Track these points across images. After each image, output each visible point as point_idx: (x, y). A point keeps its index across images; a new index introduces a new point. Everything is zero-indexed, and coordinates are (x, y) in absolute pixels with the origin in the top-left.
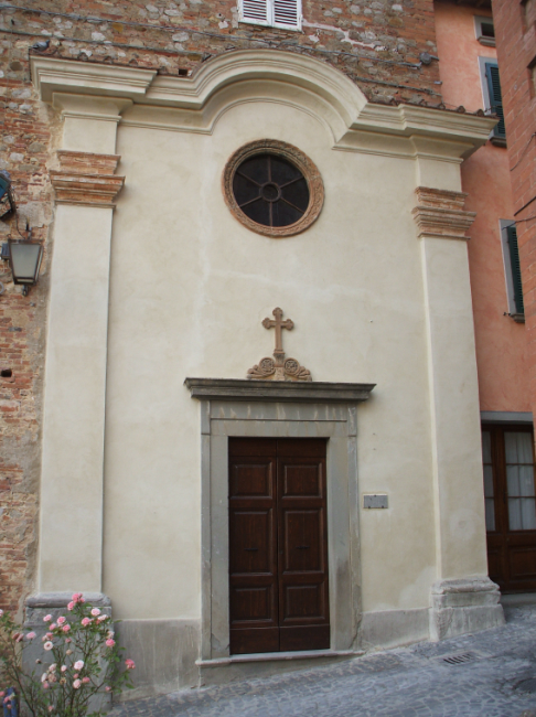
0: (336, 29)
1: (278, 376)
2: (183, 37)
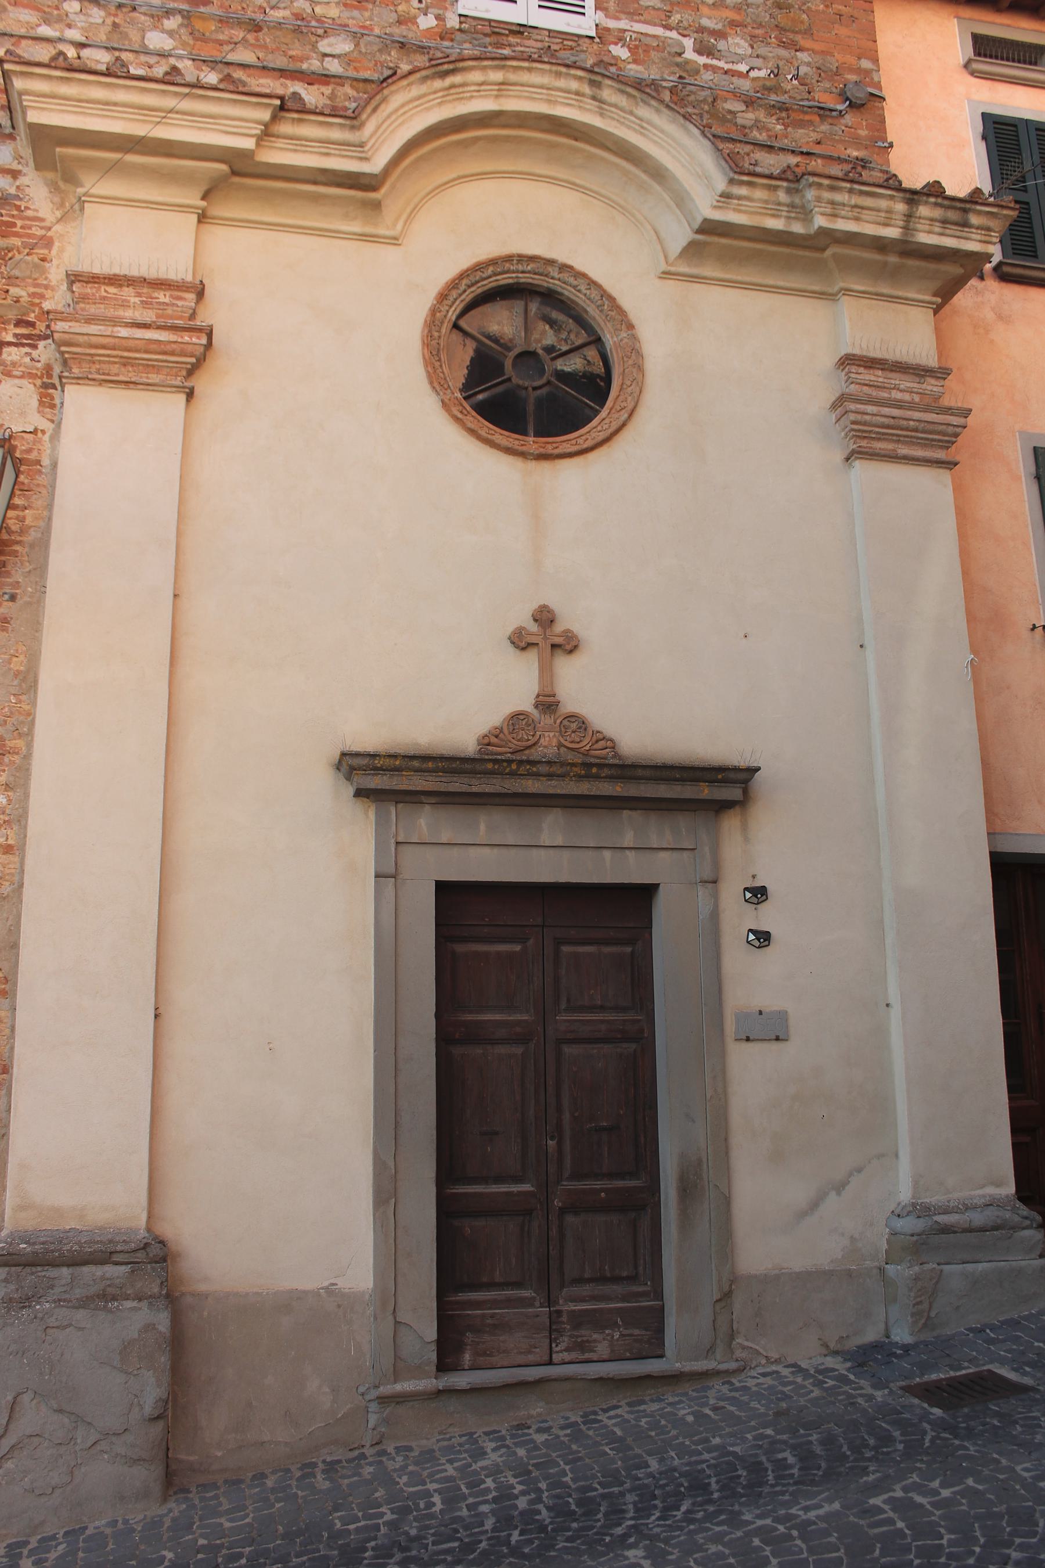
0: (668, 34)
1: (548, 745)
2: (342, 45)
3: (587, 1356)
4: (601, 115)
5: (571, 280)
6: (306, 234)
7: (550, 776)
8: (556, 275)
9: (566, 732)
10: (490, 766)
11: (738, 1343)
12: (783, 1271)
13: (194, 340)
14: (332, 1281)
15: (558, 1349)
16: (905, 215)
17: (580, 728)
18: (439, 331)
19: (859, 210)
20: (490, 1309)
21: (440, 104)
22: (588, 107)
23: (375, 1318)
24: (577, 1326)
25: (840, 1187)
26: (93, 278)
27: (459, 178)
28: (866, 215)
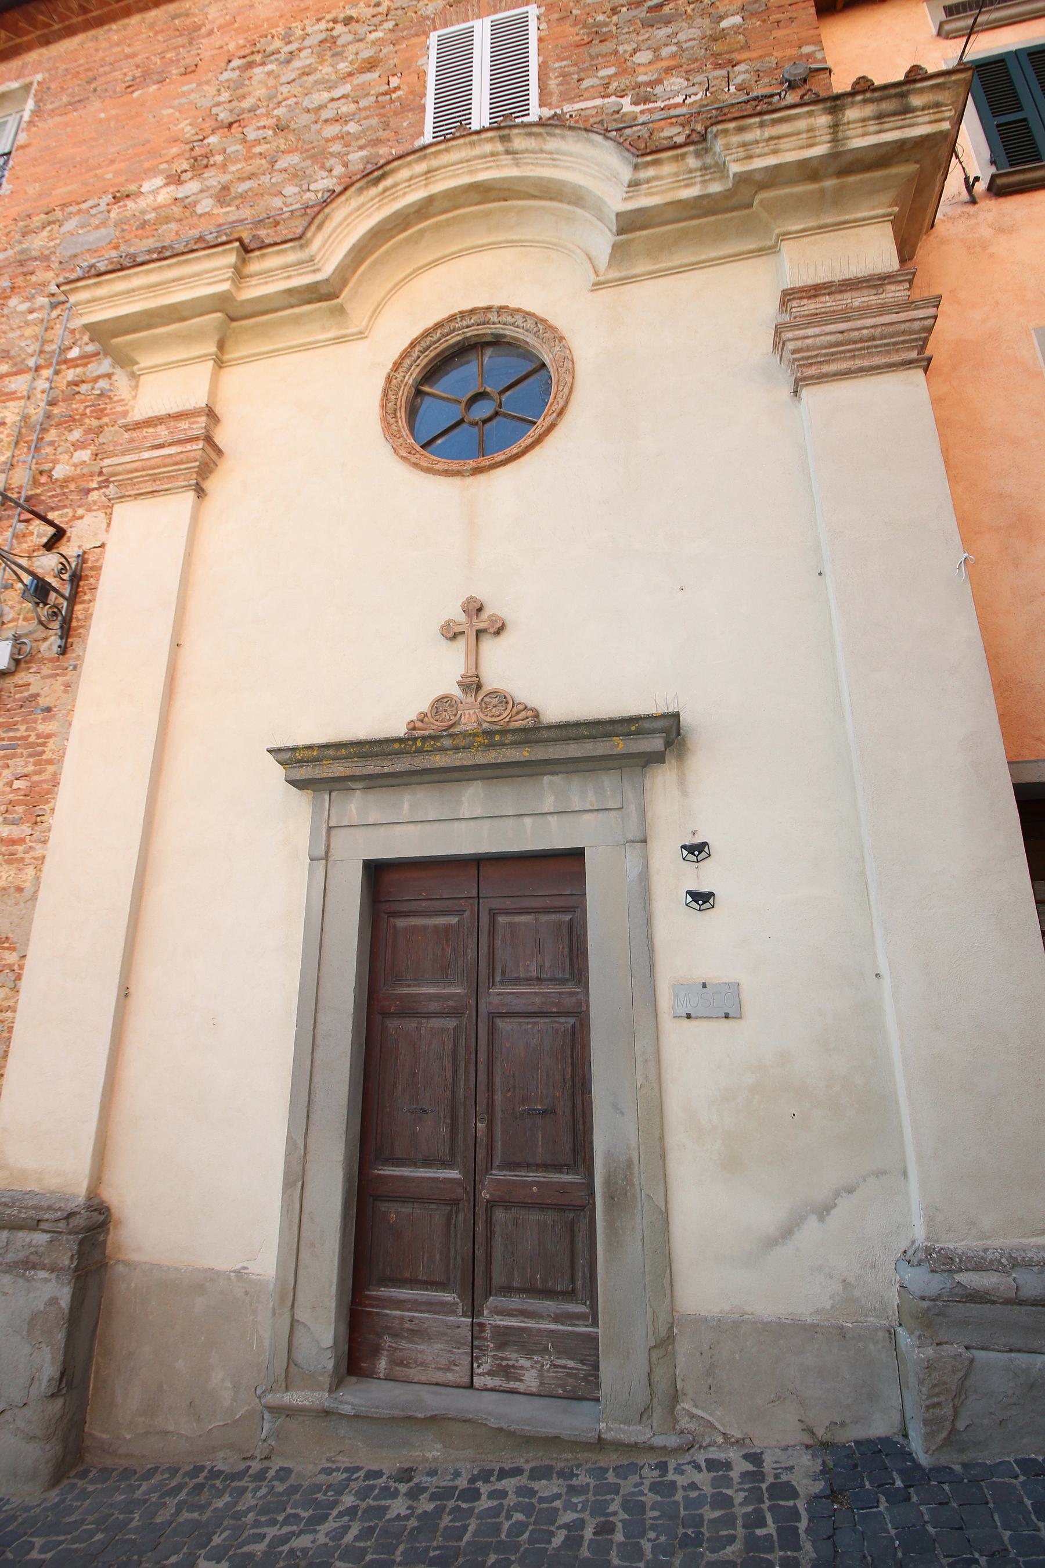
1: (470, 719)
3: (512, 1385)
4: (517, 165)
5: (509, 319)
6: (296, 352)
7: (456, 749)
8: (496, 321)
9: (486, 708)
10: (396, 746)
11: (684, 1409)
12: (746, 1316)
13: (195, 447)
14: (245, 1264)
15: (480, 1371)
16: (830, 127)
17: (501, 702)
18: (397, 394)
19: (776, 141)
20: (410, 1310)
21: (379, 208)
22: (504, 163)
23: (274, 1314)
24: (501, 1346)
25: (824, 1211)
26: (136, 424)
27: (415, 271)
28: (784, 144)
